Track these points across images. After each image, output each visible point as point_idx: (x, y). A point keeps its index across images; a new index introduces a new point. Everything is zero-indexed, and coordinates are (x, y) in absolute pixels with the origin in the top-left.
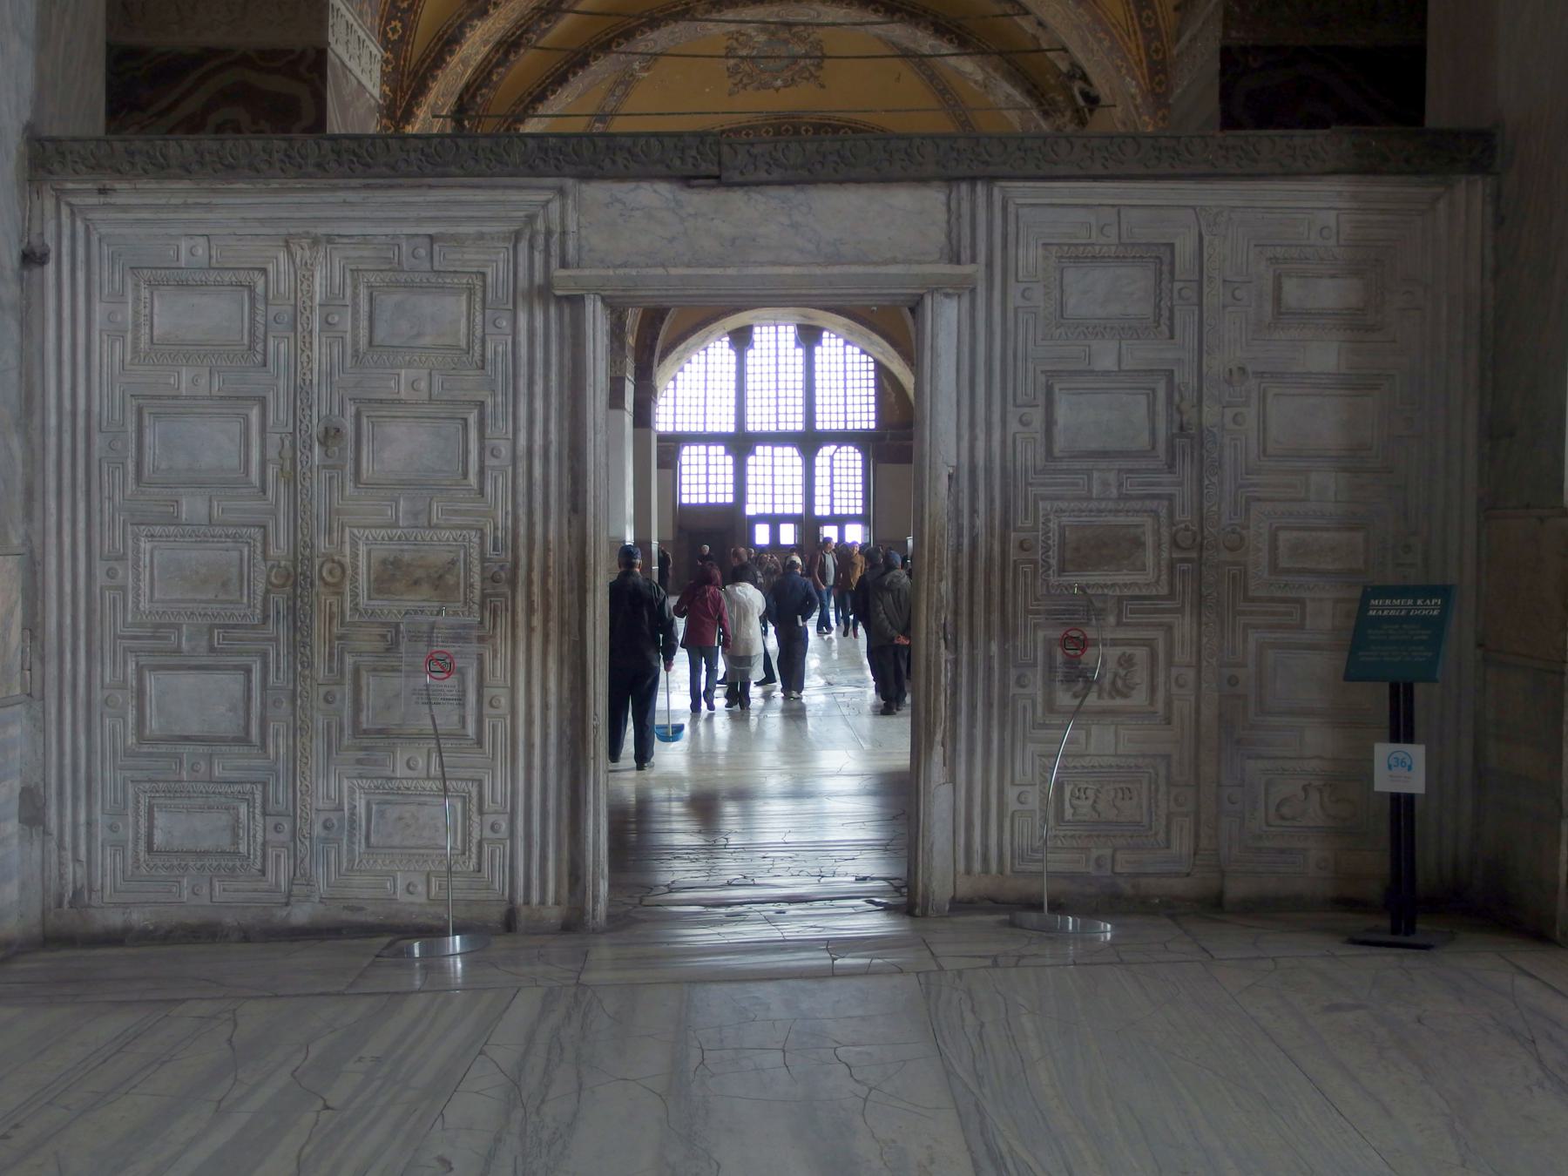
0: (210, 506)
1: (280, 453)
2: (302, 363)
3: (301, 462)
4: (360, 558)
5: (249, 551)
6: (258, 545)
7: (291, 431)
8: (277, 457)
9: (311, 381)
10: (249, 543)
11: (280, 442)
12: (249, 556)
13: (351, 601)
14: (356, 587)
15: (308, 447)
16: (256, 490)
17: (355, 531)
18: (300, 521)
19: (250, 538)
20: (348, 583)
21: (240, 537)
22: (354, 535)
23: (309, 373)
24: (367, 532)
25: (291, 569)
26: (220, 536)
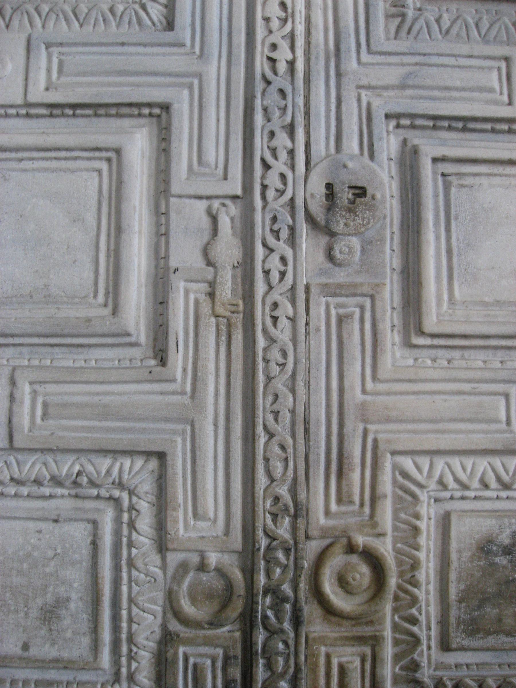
0: (12, 398)
1: (206, 252)
2: (267, 20)
3: (267, 273)
4: (422, 540)
5: (118, 520)
6: (144, 506)
7: (239, 192)
8: (199, 262)
9: (291, 64)
10: (117, 501)
11: (205, 222)
12: (117, 533)
13: (397, 658)
14: (414, 621)
15: (285, 234)
16: (136, 353)
17: (408, 463)
18: (262, 439)
19: (121, 485)
20: (388, 607)
21: (92, 483)
22: (406, 475)
23: (284, 45)
24: (440, 464)
25: (237, 576)
26: (38, 482)
